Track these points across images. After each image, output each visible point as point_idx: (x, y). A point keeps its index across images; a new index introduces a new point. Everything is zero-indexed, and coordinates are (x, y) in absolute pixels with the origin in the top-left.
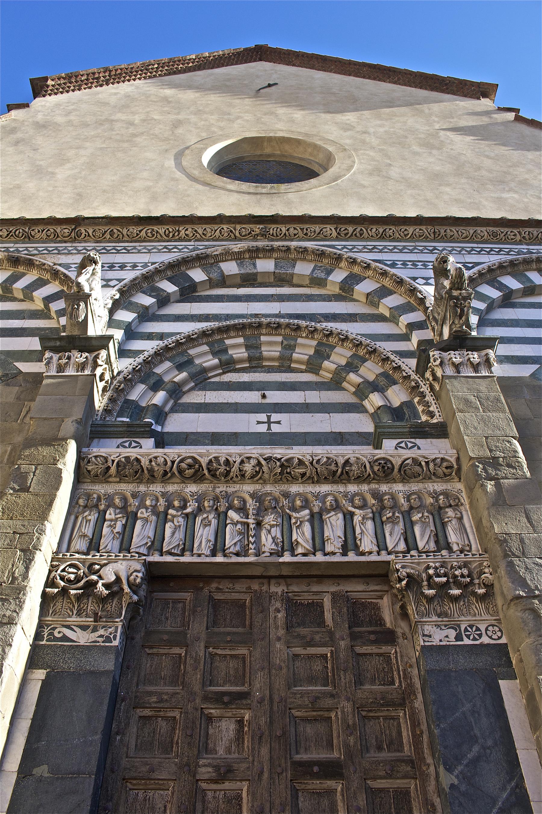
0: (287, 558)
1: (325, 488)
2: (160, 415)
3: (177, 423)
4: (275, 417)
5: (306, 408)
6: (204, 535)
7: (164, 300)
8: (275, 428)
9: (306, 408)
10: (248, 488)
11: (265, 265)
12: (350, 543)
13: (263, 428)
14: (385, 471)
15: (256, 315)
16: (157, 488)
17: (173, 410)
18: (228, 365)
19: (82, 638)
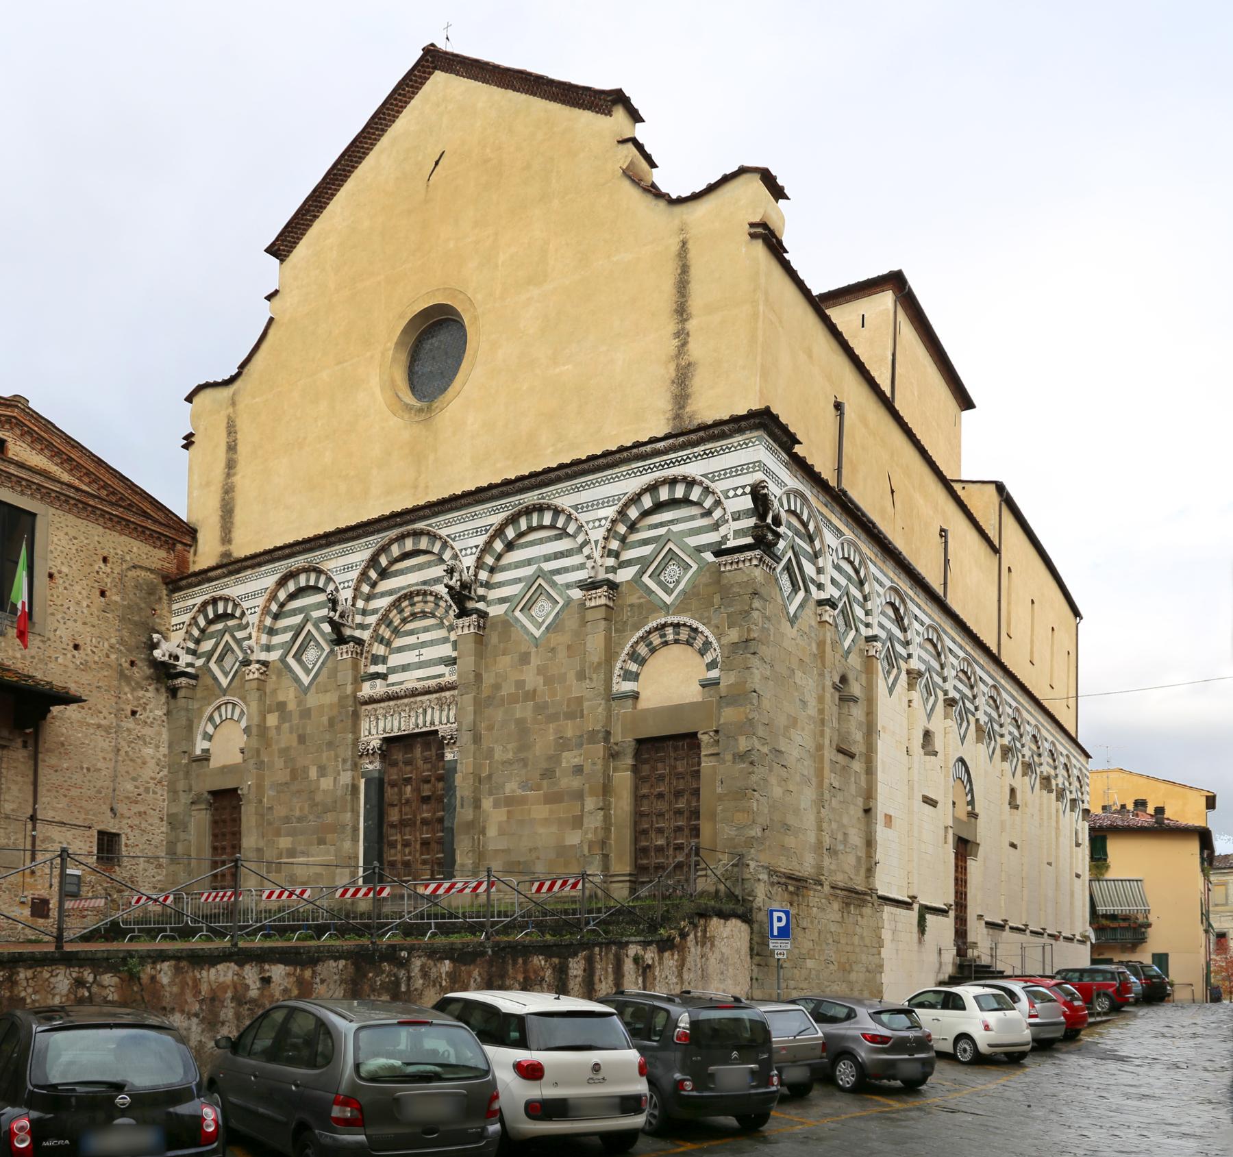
0: (417, 731)
1: (427, 697)
2: (384, 660)
3: (395, 660)
4: (422, 651)
5: (432, 643)
6: (396, 723)
7: (374, 585)
8: (422, 658)
9: (432, 643)
10: (406, 701)
11: (409, 545)
12: (432, 723)
13: (417, 660)
14: (441, 689)
15: (409, 586)
16: (382, 705)
17: (390, 653)
18: (404, 621)
19: (370, 767)
